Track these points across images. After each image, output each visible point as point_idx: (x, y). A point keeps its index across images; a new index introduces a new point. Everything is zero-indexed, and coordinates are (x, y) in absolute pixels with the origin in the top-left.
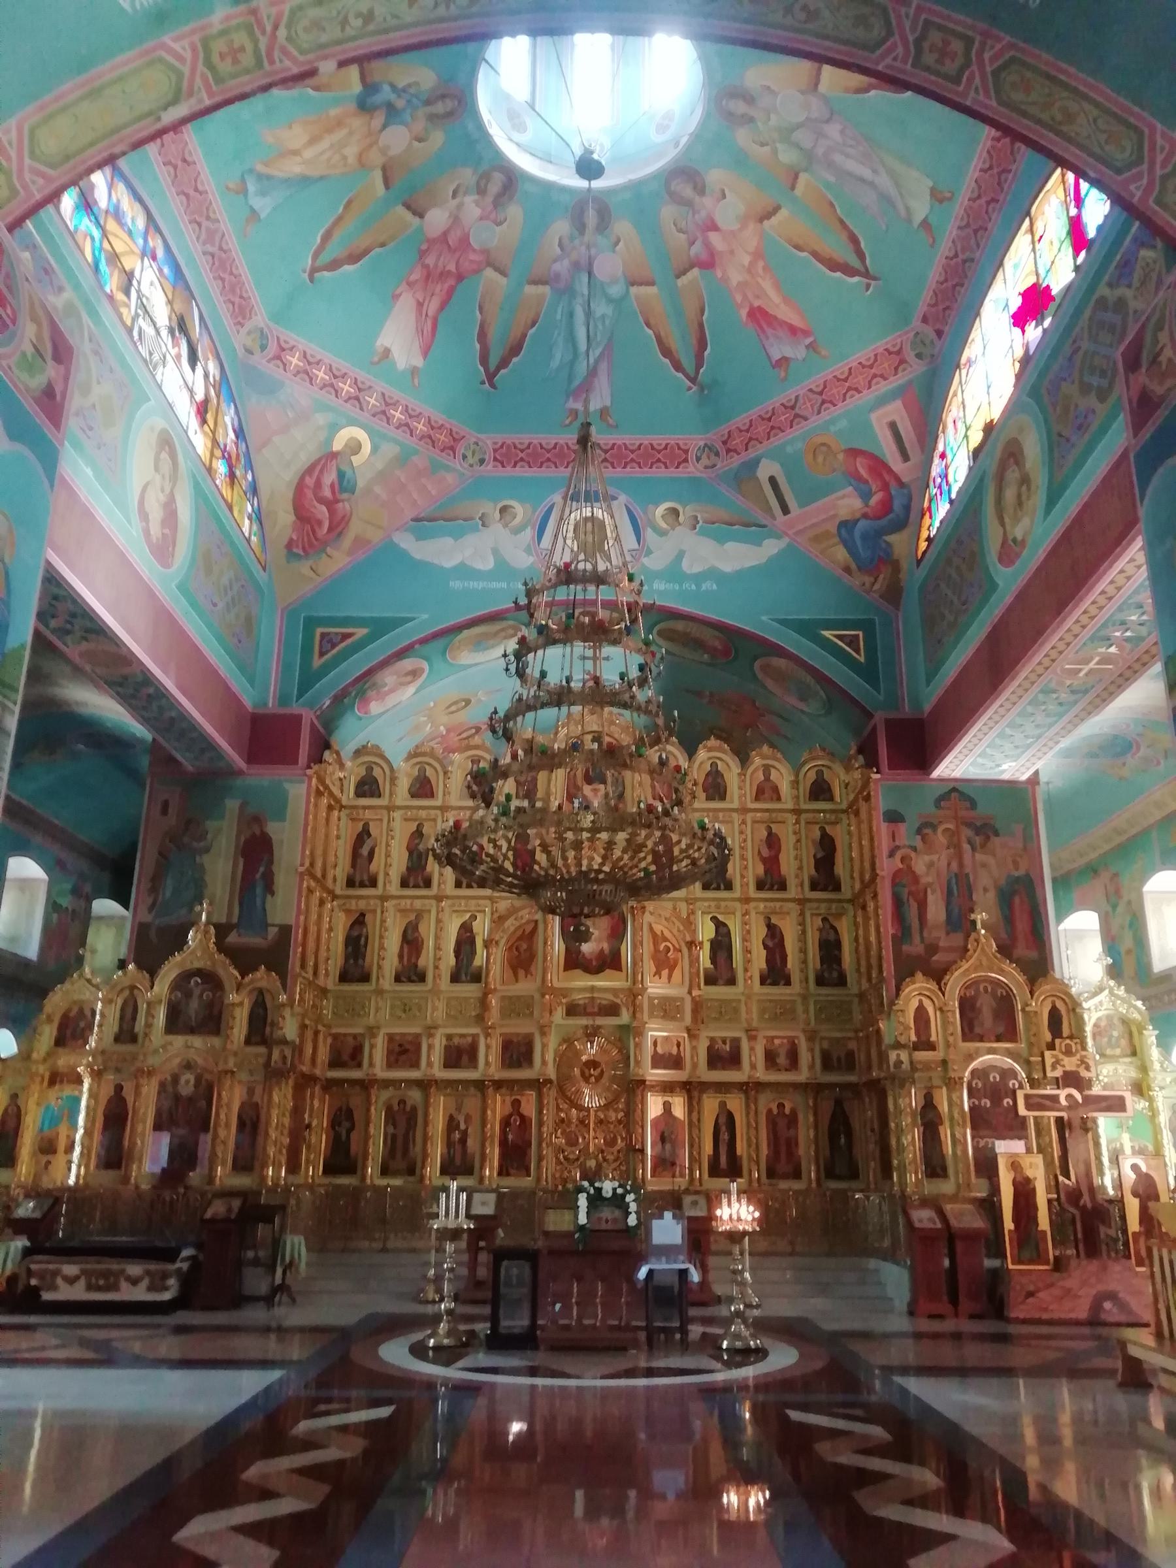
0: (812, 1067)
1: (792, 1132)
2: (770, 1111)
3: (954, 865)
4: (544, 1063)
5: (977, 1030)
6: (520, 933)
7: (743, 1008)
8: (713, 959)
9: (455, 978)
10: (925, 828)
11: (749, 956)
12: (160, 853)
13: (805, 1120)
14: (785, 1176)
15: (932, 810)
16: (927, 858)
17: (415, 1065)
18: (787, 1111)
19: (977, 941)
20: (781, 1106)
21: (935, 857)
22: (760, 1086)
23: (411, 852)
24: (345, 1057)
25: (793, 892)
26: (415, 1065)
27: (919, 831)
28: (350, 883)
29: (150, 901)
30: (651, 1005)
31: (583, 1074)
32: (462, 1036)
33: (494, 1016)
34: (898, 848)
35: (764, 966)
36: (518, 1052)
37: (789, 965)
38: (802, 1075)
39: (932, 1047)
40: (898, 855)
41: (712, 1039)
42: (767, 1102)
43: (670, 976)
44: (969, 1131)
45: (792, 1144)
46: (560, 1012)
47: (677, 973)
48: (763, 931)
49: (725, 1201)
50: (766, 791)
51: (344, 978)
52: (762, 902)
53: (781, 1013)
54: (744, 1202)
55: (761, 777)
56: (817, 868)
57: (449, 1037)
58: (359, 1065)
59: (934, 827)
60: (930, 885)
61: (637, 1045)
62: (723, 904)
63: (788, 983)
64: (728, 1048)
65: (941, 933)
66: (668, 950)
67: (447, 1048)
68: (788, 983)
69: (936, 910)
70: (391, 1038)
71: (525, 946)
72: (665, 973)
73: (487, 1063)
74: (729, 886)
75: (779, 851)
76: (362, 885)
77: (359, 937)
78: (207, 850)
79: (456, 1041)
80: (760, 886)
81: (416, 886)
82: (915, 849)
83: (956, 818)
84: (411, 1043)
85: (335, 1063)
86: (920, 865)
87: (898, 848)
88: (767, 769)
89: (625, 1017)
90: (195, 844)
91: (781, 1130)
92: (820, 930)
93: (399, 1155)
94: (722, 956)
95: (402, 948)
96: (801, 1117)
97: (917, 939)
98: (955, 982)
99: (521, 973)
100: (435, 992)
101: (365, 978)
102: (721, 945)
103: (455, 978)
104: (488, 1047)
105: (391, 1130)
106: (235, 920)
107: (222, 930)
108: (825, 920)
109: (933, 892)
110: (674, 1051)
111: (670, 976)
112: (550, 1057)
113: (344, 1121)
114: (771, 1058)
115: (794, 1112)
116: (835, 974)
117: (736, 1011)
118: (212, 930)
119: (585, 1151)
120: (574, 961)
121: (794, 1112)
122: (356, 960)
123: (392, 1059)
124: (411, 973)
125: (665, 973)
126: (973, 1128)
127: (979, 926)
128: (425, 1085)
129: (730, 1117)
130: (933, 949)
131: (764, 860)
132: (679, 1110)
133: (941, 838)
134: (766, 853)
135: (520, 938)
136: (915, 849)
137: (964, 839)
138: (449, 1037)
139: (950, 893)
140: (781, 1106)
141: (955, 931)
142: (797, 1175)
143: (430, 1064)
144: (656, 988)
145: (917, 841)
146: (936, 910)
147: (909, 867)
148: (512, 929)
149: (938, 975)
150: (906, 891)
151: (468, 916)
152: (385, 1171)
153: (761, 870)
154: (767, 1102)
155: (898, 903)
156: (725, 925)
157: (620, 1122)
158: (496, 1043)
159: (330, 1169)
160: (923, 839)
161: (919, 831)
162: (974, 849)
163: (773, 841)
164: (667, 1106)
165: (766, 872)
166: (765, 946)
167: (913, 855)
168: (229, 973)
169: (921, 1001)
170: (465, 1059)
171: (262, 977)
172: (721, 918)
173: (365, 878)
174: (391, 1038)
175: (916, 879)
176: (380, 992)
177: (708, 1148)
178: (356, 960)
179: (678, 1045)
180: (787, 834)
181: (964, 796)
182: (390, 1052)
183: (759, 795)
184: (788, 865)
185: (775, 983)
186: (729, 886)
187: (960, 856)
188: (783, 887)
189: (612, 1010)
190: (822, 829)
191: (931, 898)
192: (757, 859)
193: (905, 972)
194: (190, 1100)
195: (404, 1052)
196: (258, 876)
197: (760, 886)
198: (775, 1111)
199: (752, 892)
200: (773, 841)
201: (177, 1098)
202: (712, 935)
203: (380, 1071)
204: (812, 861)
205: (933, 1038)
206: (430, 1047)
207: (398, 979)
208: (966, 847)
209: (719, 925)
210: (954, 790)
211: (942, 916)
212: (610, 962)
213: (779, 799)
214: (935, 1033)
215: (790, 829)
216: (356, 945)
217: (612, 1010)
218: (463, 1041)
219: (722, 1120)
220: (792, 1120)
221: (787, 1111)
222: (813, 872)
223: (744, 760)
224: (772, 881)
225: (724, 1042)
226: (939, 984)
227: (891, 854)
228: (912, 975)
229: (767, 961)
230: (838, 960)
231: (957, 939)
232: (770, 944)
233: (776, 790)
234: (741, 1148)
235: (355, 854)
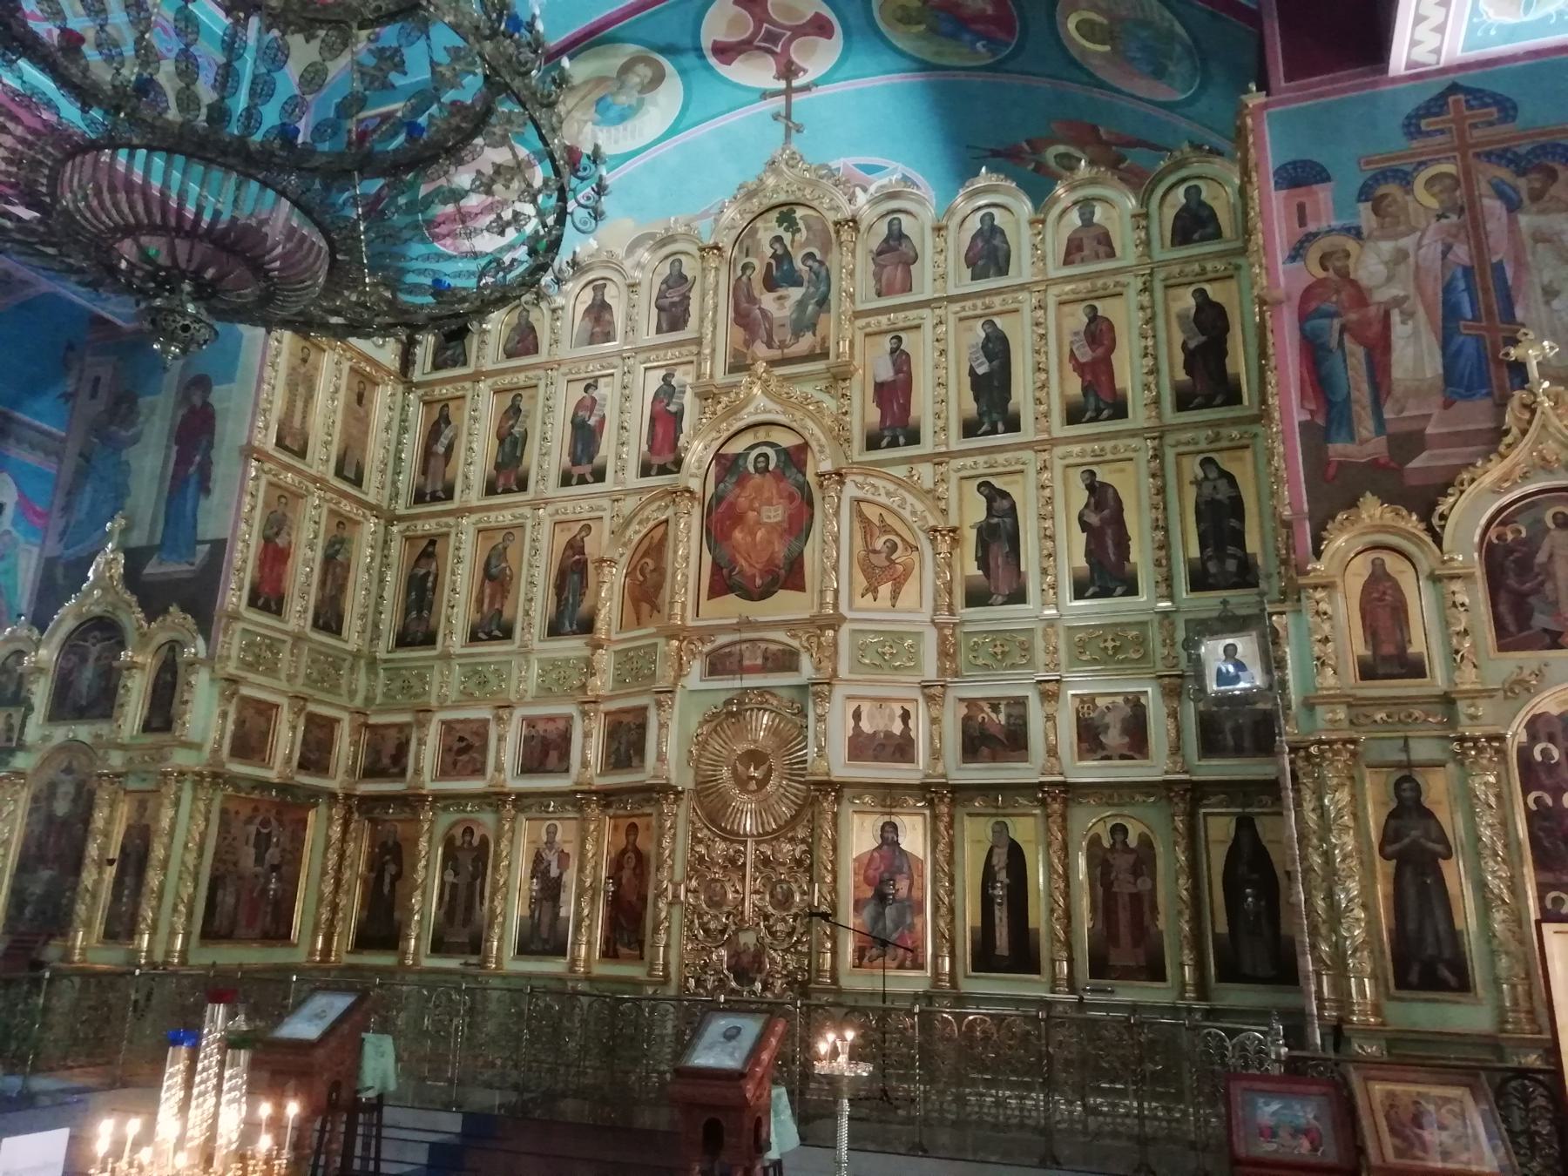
0: (1177, 749)
1: (1143, 884)
2: (1095, 842)
3: (1462, 253)
4: (661, 758)
5: (1540, 620)
6: (646, 543)
7: (1039, 643)
8: (983, 562)
9: (554, 630)
10: (1380, 186)
11: (1054, 545)
12: (81, 455)
13: (1170, 859)
14: (1128, 974)
15: (1397, 142)
16: (1387, 247)
17: (479, 771)
18: (1132, 841)
19: (1531, 408)
20: (1119, 830)
21: (1407, 242)
22: (1070, 792)
23: (502, 441)
24: (386, 761)
25: (1139, 415)
26: (479, 771)
27: (1365, 193)
28: (419, 497)
29: (61, 523)
30: (860, 650)
31: (735, 771)
32: (551, 719)
33: (601, 683)
34: (1311, 237)
35: (1081, 562)
36: (626, 740)
37: (1134, 557)
38: (1155, 767)
39: (1416, 669)
40: (1314, 253)
41: (971, 703)
42: (1090, 821)
43: (895, 595)
44: (1529, 871)
45: (1142, 905)
46: (696, 667)
47: (910, 590)
48: (1081, 497)
49: (174, 1072)
50: (1089, 244)
51: (403, 641)
52: (1079, 445)
53: (1112, 647)
54: (236, 1077)
55: (1075, 218)
56: (1189, 367)
57: (530, 722)
58: (403, 773)
59: (1405, 180)
60: (1398, 302)
61: (821, 718)
62: (1001, 458)
63: (1132, 590)
64: (1002, 718)
65: (1434, 407)
66: (894, 547)
67: (528, 740)
68: (1132, 590)
69: (1415, 354)
70: (448, 726)
71: (651, 564)
72: (885, 589)
73: (585, 764)
74: (1013, 425)
75: (1112, 348)
76: (435, 498)
77: (428, 574)
78: (135, 440)
79: (541, 727)
80: (1074, 415)
81: (507, 491)
82: (1357, 233)
83: (1463, 148)
84: (477, 734)
85: (371, 773)
86: (1370, 266)
87: (1311, 237)
88: (1086, 205)
89: (808, 668)
90: (123, 433)
91: (1120, 878)
92: (1198, 483)
93: (459, 917)
94: (999, 551)
95: (482, 585)
96: (1160, 849)
97: (1366, 428)
98: (1469, 514)
99: (645, 607)
100: (525, 652)
101: (429, 640)
102: (999, 534)
103: (554, 630)
104: (587, 735)
105: (450, 878)
106: (157, 541)
107: (135, 558)
108: (1207, 462)
109: (1408, 316)
110: (897, 728)
111: (895, 595)
112: (672, 749)
113: (388, 868)
114: (1090, 736)
115: (1146, 843)
116: (1231, 565)
117: (1026, 649)
118: (122, 559)
119: (737, 912)
120: (723, 582)
121: (1146, 843)
122: (420, 611)
123: (449, 760)
124: (493, 627)
125: (885, 589)
126: (1541, 864)
127: (1533, 371)
128: (495, 799)
129: (1016, 855)
130: (1409, 442)
131: (1080, 368)
132: (913, 837)
133: (1423, 197)
134: (1085, 355)
135: (646, 554)
136: (1357, 233)
137: (1483, 187)
138: (530, 722)
139: (1451, 312)
140: (1119, 830)
141: (1469, 393)
142: (1155, 972)
143: (499, 768)
144: (867, 611)
145: (1365, 216)
146: (1415, 354)
147: (1344, 274)
148: (637, 538)
149: (1425, 501)
150: (1336, 323)
151: (578, 526)
152: (439, 946)
153: (1075, 386)
154: (1090, 821)
155: (1314, 353)
156: (1005, 495)
157: (799, 862)
158: (598, 729)
159: (364, 942)
160: (1376, 211)
161: (1365, 193)
162: (1513, 206)
163: (1099, 333)
164: (889, 835)
165: (1086, 390)
166: (1085, 526)
167: (1351, 245)
168: (132, 618)
169: (1378, 566)
170: (554, 755)
171: (177, 620)
172: (998, 483)
173: (439, 486)
174: (448, 726)
175: (1360, 297)
176: (447, 657)
177: (970, 914)
178: (420, 611)
179: (906, 716)
180: (1124, 314)
181: (1476, 96)
182: (447, 750)
183: (1074, 251)
184: (1127, 372)
185: (1105, 593)
186: (1013, 425)
187: (1475, 230)
188: (1119, 410)
189: (785, 661)
190: (1201, 294)
191: (1400, 331)
192: (1069, 367)
193: (1334, 491)
194: (65, 823)
195: (464, 750)
196: (192, 469)
197: (1074, 415)
198: (1106, 843)
199: (1059, 429)
200: (1099, 333)
201: (50, 819)
202: (981, 515)
203: (430, 785)
204: (1180, 357)
205: (1416, 647)
206: (501, 738)
207: (474, 638)
208: (1493, 206)
209: (993, 495)
210: (1454, 88)
211: (1433, 367)
212: (791, 575)
213: (1111, 254)
214: (1423, 637)
215: (1134, 305)
216: (421, 592)
217: (785, 661)
218: (551, 727)
219: (1000, 859)
220: (1144, 859)
221: (1132, 841)
222: (1182, 375)
223: (1038, 189)
224: (1099, 401)
225: (995, 708)
226: (1425, 517)
227: (1297, 253)
228: (1352, 504)
229: (1089, 554)
230: (1239, 538)
231: (1474, 414)
232: (1094, 519)
233: (1105, 240)
234: (1038, 915)
235: (428, 453)
